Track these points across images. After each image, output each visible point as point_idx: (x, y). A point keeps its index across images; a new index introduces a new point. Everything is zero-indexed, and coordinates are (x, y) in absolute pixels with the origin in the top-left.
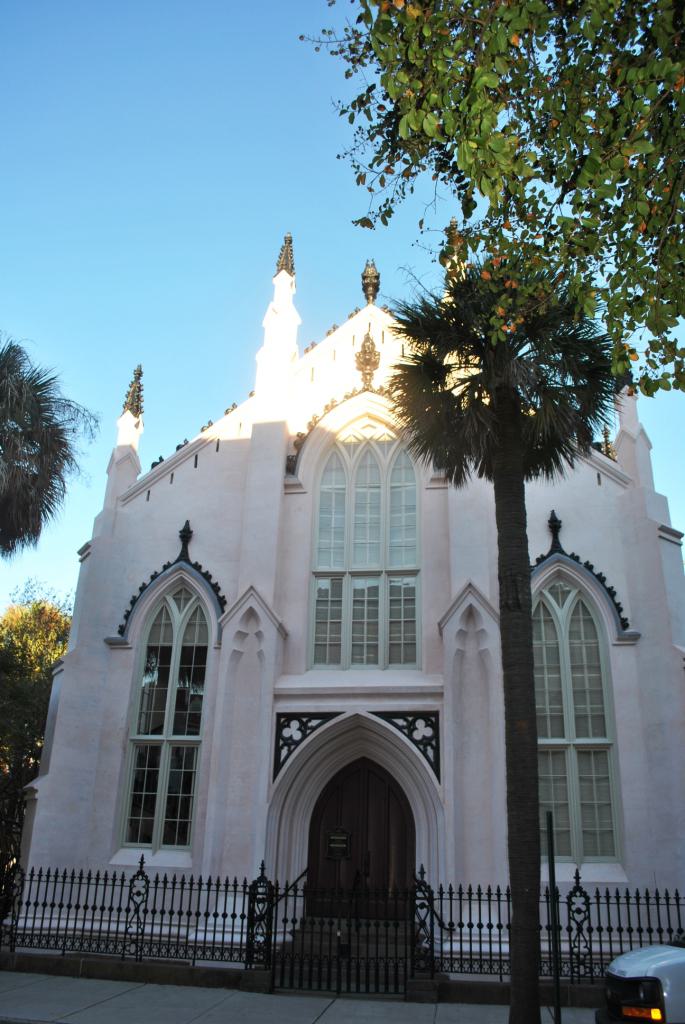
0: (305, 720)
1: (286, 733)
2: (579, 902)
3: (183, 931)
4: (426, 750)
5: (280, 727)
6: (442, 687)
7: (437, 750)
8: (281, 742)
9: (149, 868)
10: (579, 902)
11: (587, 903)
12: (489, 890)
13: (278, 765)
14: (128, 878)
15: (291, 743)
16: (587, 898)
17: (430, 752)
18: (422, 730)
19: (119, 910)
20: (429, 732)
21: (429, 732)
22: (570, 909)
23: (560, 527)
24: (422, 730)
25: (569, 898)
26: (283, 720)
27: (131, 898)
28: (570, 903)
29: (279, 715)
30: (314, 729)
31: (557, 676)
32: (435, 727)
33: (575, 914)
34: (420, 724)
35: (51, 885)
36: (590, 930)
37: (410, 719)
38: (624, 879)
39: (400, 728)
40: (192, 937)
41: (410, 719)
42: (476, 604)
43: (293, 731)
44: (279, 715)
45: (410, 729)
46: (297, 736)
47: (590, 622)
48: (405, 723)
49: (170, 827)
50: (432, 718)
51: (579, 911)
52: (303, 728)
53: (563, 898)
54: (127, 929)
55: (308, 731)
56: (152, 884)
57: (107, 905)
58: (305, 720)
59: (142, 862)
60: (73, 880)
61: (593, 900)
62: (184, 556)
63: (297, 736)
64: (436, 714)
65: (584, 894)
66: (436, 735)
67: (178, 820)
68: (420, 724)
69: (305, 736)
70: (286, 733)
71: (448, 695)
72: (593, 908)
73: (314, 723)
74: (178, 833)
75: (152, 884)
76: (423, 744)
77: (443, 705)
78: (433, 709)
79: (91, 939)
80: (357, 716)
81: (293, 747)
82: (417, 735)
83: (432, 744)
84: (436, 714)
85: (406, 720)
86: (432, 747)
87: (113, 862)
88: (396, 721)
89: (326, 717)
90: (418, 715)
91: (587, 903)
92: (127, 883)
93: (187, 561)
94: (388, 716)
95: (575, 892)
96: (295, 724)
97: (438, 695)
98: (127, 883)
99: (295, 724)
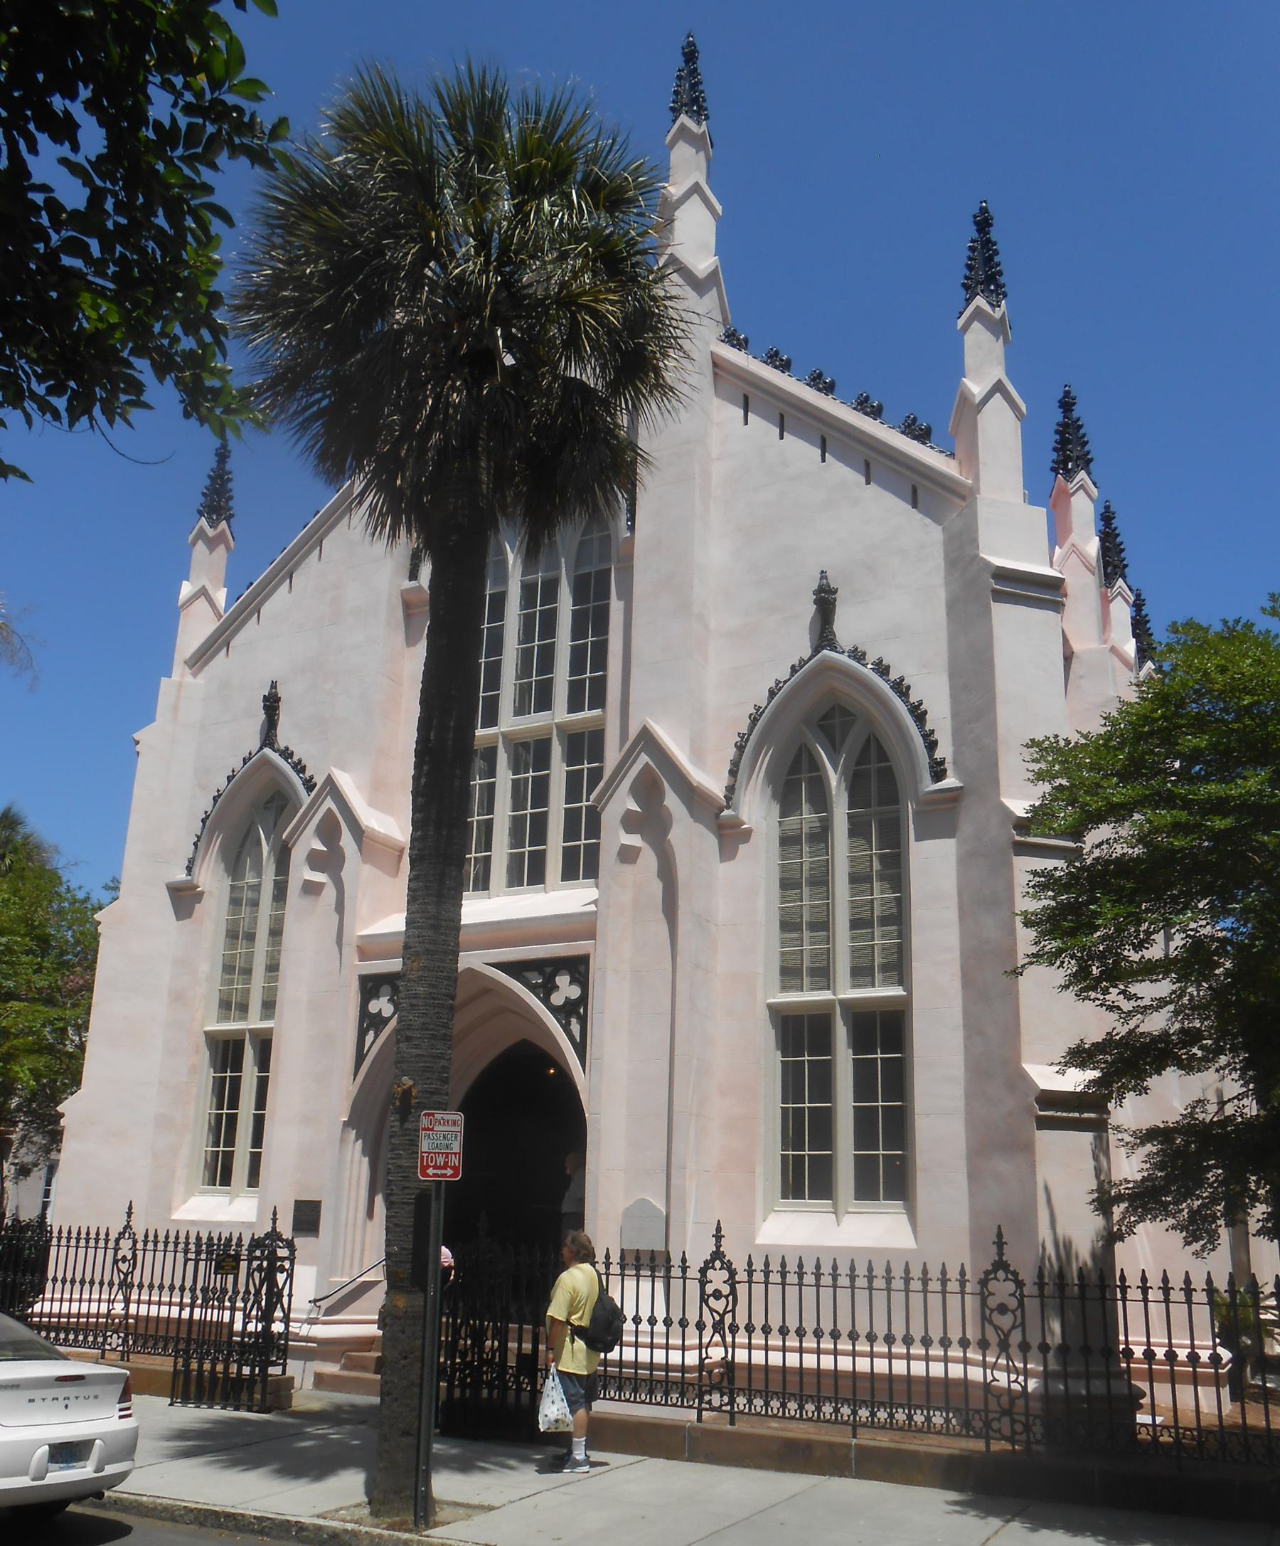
1: (374, 1007)
4: (569, 1023)
7: (583, 1021)
10: (718, 1278)
11: (732, 1282)
12: (907, 1271)
13: (360, 1057)
14: (113, 1236)
15: (377, 1022)
16: (733, 1273)
17: (575, 1027)
20: (575, 992)
21: (575, 992)
22: (984, 1303)
24: (566, 989)
27: (704, 1299)
28: (703, 1283)
37: (548, 970)
39: (533, 988)
40: (238, 1326)
50: (578, 968)
51: (717, 1295)
53: (693, 1272)
54: (109, 1311)
56: (140, 1246)
61: (742, 1276)
65: (728, 1266)
66: (583, 999)
68: (563, 980)
70: (374, 1007)
72: (742, 1290)
75: (140, 1246)
82: (557, 999)
87: (176, 1216)
92: (111, 1244)
94: (516, 969)
98: (111, 1244)
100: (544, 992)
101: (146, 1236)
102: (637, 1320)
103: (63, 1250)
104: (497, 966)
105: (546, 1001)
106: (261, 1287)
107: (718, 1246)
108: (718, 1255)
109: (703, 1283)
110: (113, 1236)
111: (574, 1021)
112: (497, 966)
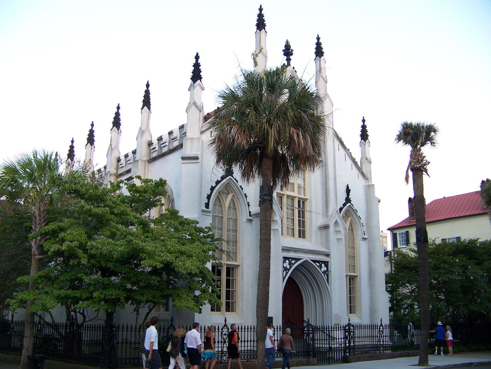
2: (381, 328)
5: (284, 262)
7: (328, 275)
8: (285, 269)
10: (381, 328)
13: (284, 279)
16: (383, 327)
17: (326, 276)
18: (324, 268)
20: (325, 269)
21: (325, 269)
24: (324, 268)
25: (380, 327)
26: (285, 258)
29: (284, 257)
30: (293, 264)
31: (235, 234)
34: (323, 265)
36: (383, 337)
39: (318, 266)
41: (321, 263)
42: (339, 221)
43: (287, 264)
45: (320, 267)
46: (288, 267)
47: (352, 230)
48: (319, 265)
49: (228, 304)
50: (326, 264)
52: (290, 264)
55: (292, 265)
56: (276, 330)
58: (290, 260)
61: (384, 328)
63: (288, 267)
64: (328, 262)
65: (382, 326)
67: (231, 301)
68: (323, 265)
69: (291, 267)
70: (285, 265)
72: (384, 330)
73: (293, 262)
74: (230, 307)
75: (276, 330)
76: (324, 272)
83: (327, 272)
85: (319, 264)
86: (327, 275)
88: (317, 264)
89: (297, 260)
90: (323, 262)
91: (383, 329)
94: (315, 261)
96: (287, 261)
99: (287, 261)
103: (243, 333)
104: (312, 260)
105: (320, 269)
106: (307, 337)
107: (381, 322)
108: (381, 324)
110: (220, 328)
111: (325, 275)
112: (311, 260)
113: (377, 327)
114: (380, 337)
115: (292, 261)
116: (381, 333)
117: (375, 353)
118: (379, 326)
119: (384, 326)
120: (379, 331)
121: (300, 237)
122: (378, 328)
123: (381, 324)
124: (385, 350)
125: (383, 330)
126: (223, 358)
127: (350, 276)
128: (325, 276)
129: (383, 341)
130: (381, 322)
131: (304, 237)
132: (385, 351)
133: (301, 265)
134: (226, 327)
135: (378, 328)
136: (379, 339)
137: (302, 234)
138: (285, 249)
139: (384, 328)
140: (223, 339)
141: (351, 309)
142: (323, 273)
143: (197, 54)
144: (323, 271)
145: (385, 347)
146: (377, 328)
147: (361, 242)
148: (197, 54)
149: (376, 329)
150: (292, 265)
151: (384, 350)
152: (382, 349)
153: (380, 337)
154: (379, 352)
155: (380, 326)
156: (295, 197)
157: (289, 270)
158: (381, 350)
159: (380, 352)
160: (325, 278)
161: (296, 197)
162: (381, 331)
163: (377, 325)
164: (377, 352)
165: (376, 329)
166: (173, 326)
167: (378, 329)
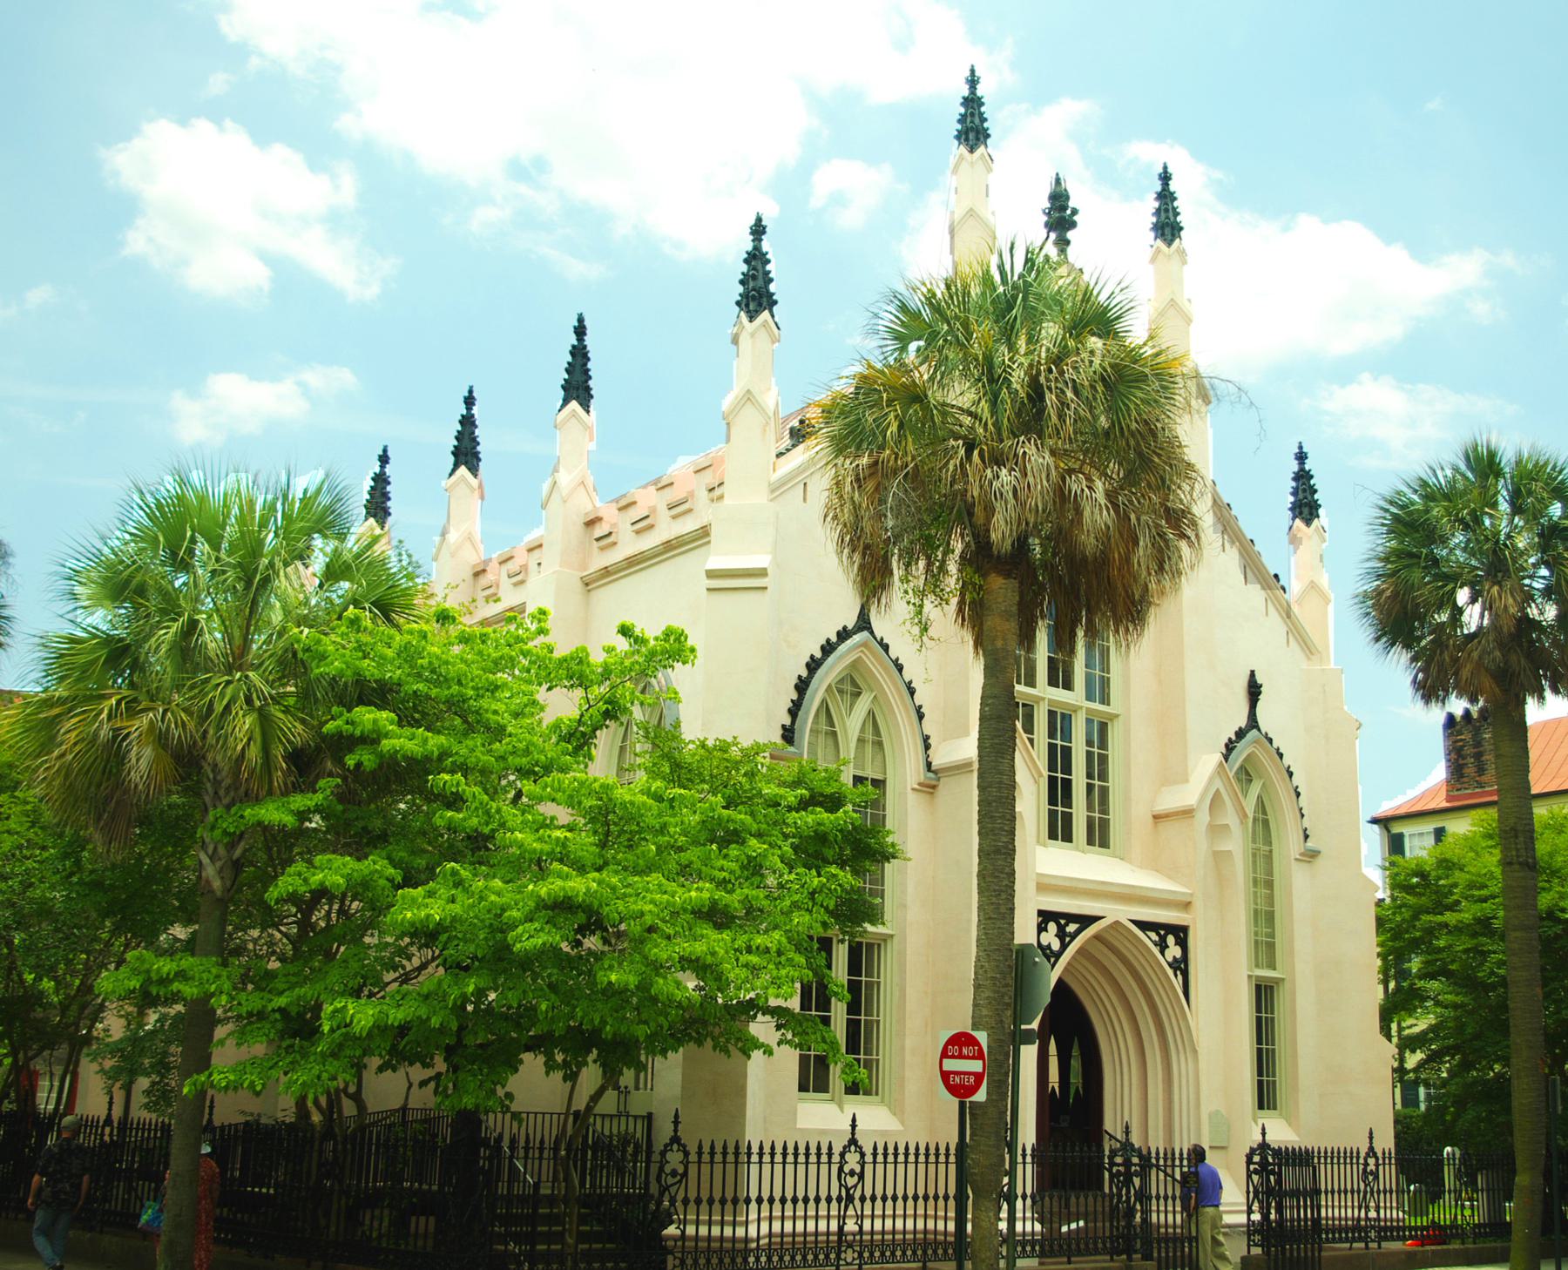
0: (1063, 922)
2: (1371, 1161)
3: (777, 1227)
5: (1041, 928)
6: (1191, 895)
9: (866, 1132)
10: (1371, 1161)
16: (1377, 1159)
17: (1180, 977)
18: (1174, 951)
19: (829, 1199)
23: (1260, 693)
25: (1366, 1159)
29: (1041, 913)
30: (1074, 936)
32: (1183, 943)
33: (848, 1177)
34: (1171, 940)
35: (901, 1168)
36: (1379, 1192)
38: (1297, 1139)
42: (1222, 791)
44: (1041, 913)
45: (1163, 946)
46: (1056, 945)
47: (1266, 823)
50: (1181, 934)
52: (1061, 934)
57: (801, 1195)
58: (1063, 922)
59: (854, 1126)
60: (724, 1157)
61: (1381, 1162)
62: (864, 623)
63: (1056, 945)
64: (1185, 929)
68: (1171, 940)
69: (1064, 947)
71: (1198, 904)
72: (1381, 1168)
73: (1072, 928)
77: (1194, 919)
78: (1185, 924)
79: (770, 1249)
80: (1117, 922)
81: (1052, 960)
83: (1181, 966)
84: (1185, 929)
85: (1158, 934)
89: (1086, 921)
91: (1377, 1165)
93: (872, 633)
94: (1144, 926)
95: (849, 1146)
96: (1052, 927)
97: (1186, 906)
99: (1052, 927)
100: (1163, 946)
101: (875, 1148)
102: (1158, 1197)
104: (1134, 922)
105: (1162, 953)
107: (1371, 1143)
108: (1371, 1149)
109: (1366, 1164)
110: (837, 1149)
112: (1134, 922)
113: (1358, 1158)
114: (1365, 1192)
115: (1067, 924)
116: (1371, 1178)
117: (1351, 1248)
118: (1362, 1155)
119: (1380, 1155)
120: (1365, 1170)
121: (1090, 842)
122: (1361, 1161)
123: (1371, 1149)
124: (1386, 1239)
125: (1377, 1169)
126: (843, 1256)
127: (1257, 977)
128: (1176, 975)
129: (1377, 1209)
130: (1371, 1143)
131: (1104, 844)
132: (1384, 1244)
133: (1097, 937)
134: (856, 1145)
135: (1361, 1161)
136: (1365, 1197)
137: (1099, 835)
138: (1045, 886)
139: (1381, 1162)
140: (846, 1187)
141: (1266, 1097)
142: (1170, 965)
143: (759, 220)
144: (1170, 959)
145: (1385, 1229)
146: (1358, 1163)
147: (1295, 866)
148: (759, 220)
149: (1355, 1166)
150: (1068, 939)
151: (1380, 1239)
152: (1373, 1234)
153: (1365, 1192)
154: (1362, 1245)
155: (1368, 1154)
156: (1076, 709)
157: (1058, 955)
158: (1373, 1241)
159: (1367, 1247)
160: (1177, 983)
161: (1081, 707)
162: (1371, 1173)
163: (1358, 1153)
164: (1355, 1245)
165: (1355, 1166)
166: (856, 1145)
167: (1361, 1167)
